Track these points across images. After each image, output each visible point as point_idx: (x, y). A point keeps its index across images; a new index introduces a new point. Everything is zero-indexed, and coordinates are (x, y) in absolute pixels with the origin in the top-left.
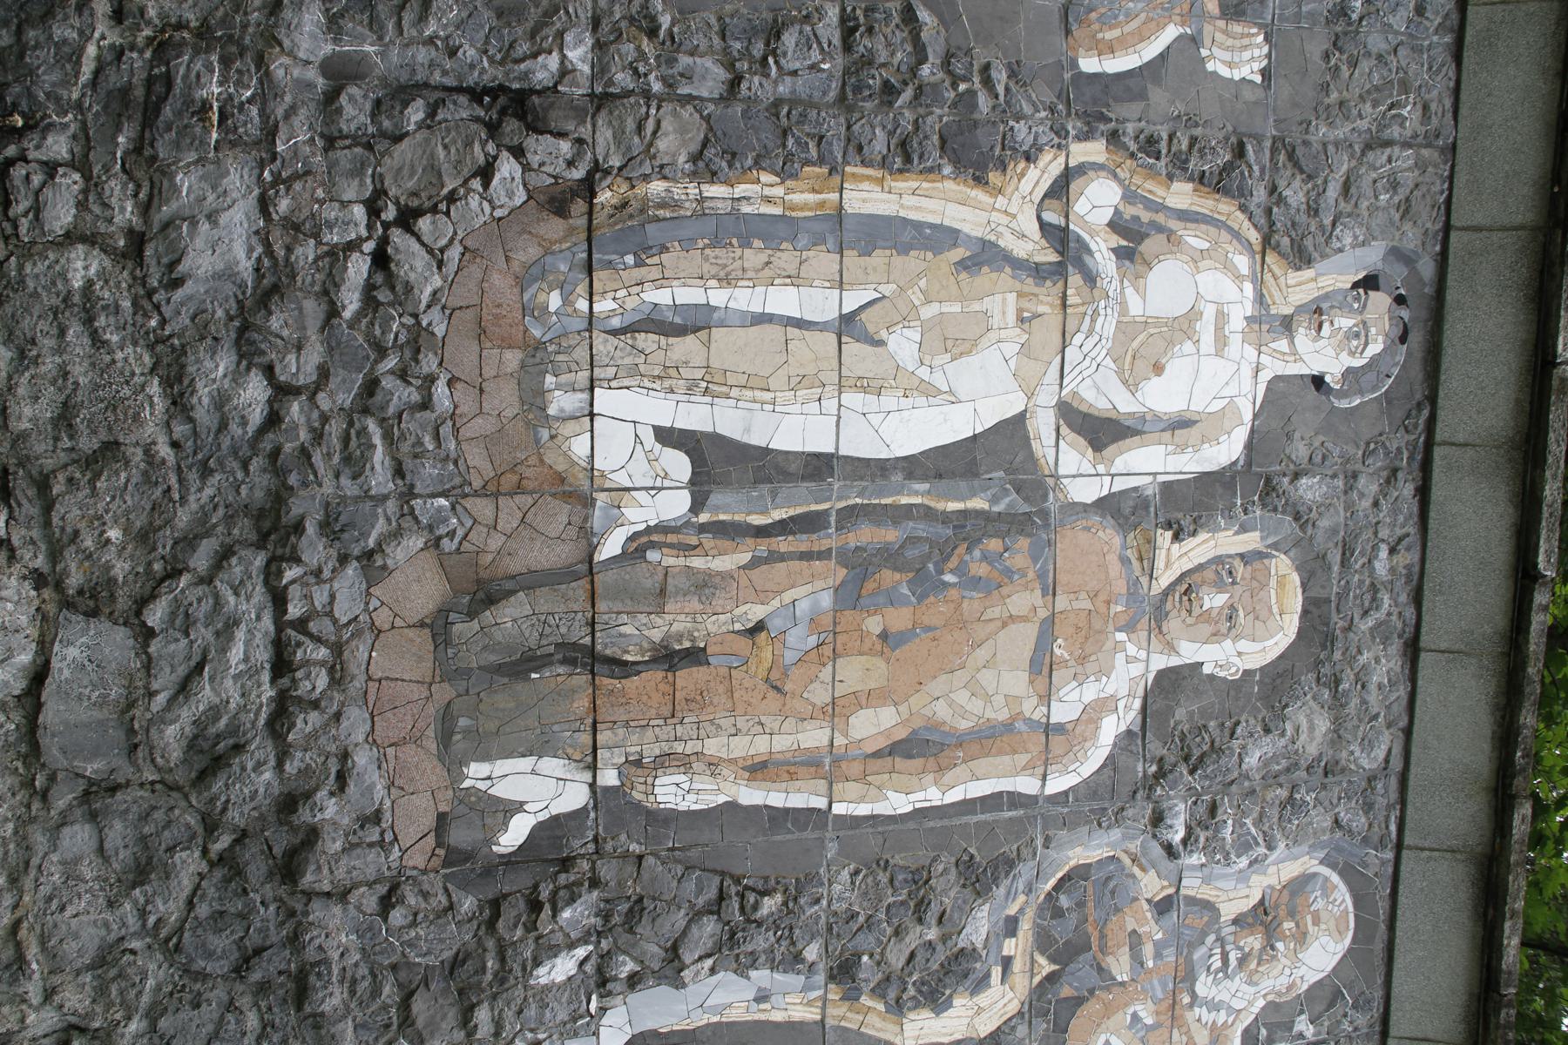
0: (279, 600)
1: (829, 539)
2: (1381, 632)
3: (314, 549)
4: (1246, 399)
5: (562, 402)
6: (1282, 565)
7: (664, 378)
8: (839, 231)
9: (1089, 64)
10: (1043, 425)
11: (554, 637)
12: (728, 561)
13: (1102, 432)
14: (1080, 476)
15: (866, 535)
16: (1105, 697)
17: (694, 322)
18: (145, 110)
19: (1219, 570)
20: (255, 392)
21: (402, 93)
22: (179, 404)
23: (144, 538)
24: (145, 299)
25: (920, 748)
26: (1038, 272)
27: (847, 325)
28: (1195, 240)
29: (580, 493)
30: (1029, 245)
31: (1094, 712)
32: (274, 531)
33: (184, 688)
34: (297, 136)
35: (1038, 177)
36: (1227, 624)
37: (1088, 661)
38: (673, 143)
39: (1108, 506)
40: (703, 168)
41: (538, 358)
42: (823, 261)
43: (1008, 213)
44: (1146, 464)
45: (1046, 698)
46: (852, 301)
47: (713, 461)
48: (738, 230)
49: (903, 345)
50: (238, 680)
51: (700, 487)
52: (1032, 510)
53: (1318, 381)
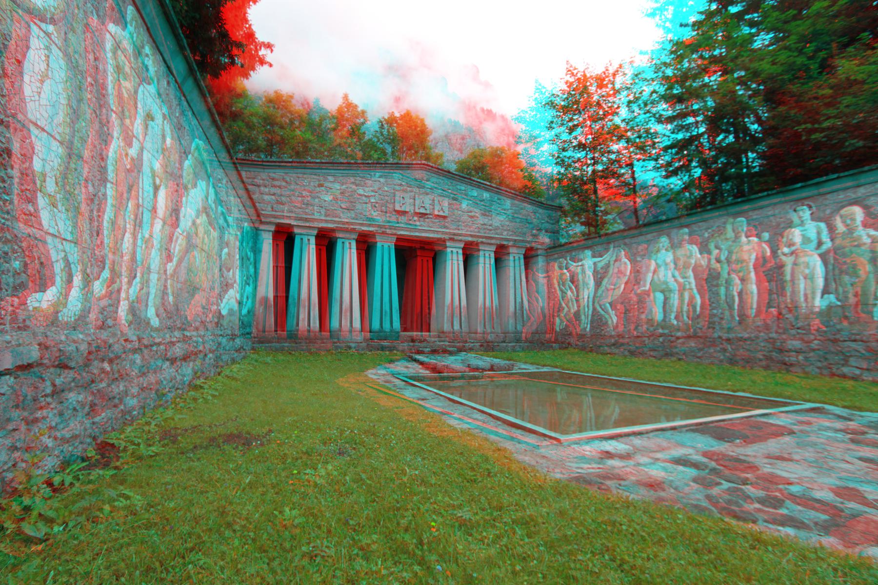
0: (845, 341)
1: (837, 277)
2: (855, 193)
3: (838, 336)
4: (814, 223)
5: (817, 310)
6: (843, 212)
7: (813, 298)
8: (793, 280)
9: (769, 254)
10: (819, 252)
12: (841, 290)
13: (820, 243)
14: (828, 245)
15: (837, 272)
17: (806, 295)
18: (781, 351)
19: (844, 222)
20: (816, 342)
21: (779, 327)
22: (818, 350)
23: (837, 355)
24: (804, 352)
26: (797, 256)
27: (805, 278)
28: (790, 237)
29: (830, 307)
30: (792, 258)
31: (869, 236)
32: (835, 341)
33: (859, 352)
34: (784, 336)
35: (784, 258)
36: (853, 220)
38: (781, 299)
39: (832, 240)
40: (785, 296)
41: (812, 313)
42: (796, 282)
43: (789, 261)
44: (825, 237)
45: (865, 244)
46: (801, 278)
47: (826, 291)
48: (793, 292)
49: (807, 271)
51: (829, 293)
52: (835, 250)
53: (811, 214)
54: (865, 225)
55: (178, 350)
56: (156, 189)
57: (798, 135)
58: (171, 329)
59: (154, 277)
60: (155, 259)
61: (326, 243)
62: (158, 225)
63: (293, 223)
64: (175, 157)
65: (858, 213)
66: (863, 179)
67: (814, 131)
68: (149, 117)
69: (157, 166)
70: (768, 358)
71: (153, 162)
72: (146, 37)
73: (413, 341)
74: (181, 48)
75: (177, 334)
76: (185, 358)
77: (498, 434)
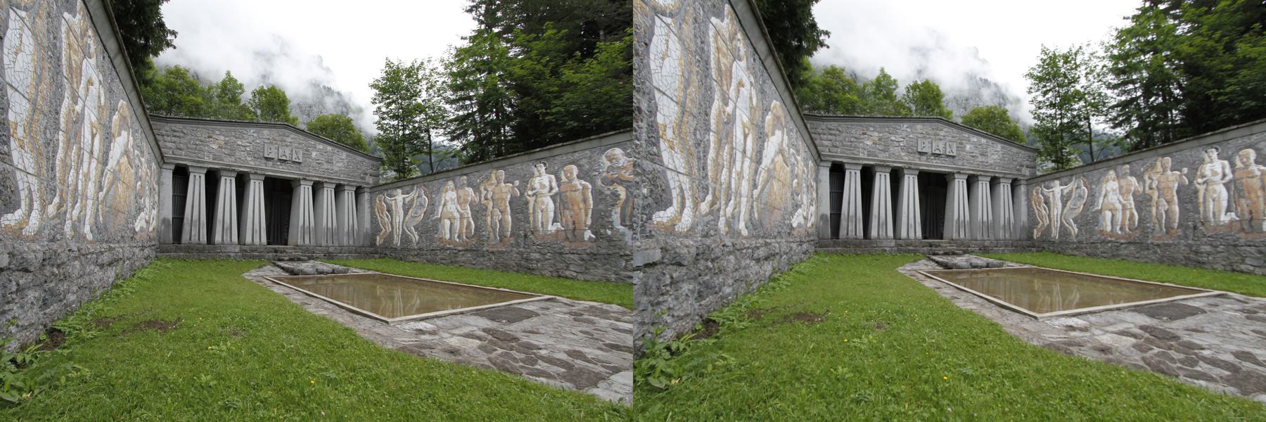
11: (574, 232)
16: (578, 183)
25: (585, 201)
37: (575, 186)
50: (576, 257)
54: (579, 177)
55: (106, 258)
56: (93, 136)
57: (537, 116)
58: (102, 241)
59: (90, 202)
60: (91, 188)
61: (212, 179)
62: (94, 164)
63: (189, 164)
64: (106, 113)
65: (575, 170)
66: (578, 147)
67: (547, 114)
68: (90, 82)
69: (94, 119)
70: (519, 265)
71: (91, 116)
72: (89, 23)
73: (276, 251)
74: (115, 33)
75: (104, 245)
76: (110, 264)
77: (343, 319)
